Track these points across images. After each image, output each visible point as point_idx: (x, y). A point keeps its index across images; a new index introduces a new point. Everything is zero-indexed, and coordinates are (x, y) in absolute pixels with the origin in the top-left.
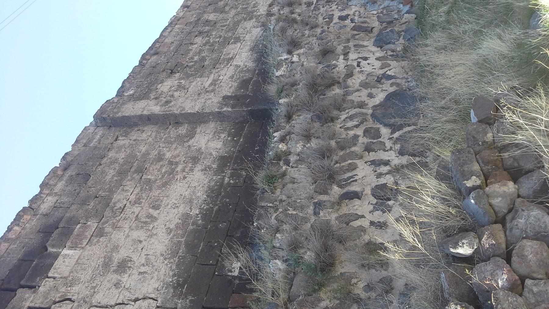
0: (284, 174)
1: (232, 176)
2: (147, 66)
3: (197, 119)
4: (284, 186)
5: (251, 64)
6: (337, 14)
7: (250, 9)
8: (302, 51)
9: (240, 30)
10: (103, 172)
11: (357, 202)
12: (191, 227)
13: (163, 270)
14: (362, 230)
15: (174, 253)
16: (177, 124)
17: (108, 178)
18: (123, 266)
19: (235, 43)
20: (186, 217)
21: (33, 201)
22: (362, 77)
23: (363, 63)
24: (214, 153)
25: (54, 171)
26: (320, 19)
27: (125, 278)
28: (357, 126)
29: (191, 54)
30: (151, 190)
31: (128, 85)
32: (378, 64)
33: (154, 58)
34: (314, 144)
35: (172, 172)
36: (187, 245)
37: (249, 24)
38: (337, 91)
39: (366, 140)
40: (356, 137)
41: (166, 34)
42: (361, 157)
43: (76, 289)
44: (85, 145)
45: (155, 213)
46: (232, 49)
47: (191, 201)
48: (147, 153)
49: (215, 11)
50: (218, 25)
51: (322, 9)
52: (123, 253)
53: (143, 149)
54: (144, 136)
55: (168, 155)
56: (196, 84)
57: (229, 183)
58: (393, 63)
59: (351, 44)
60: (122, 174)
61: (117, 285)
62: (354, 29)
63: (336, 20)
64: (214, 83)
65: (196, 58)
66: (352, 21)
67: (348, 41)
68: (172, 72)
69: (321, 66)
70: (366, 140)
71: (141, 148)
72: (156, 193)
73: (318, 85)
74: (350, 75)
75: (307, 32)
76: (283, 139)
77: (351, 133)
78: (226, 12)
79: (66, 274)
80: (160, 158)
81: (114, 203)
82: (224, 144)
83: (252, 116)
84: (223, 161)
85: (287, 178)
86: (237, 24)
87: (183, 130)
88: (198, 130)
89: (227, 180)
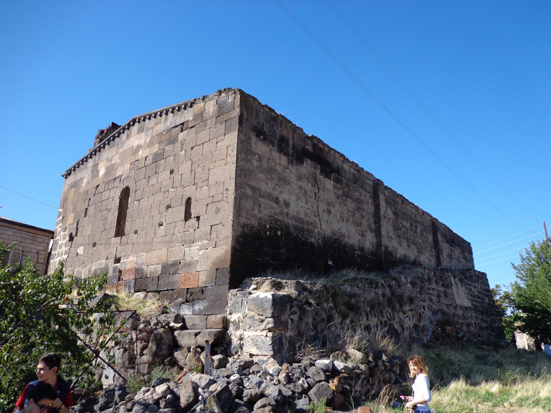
0: (372, 287)
1: (358, 254)
2: (397, 199)
3: (378, 232)
4: (369, 288)
5: (398, 256)
6: (425, 304)
7: (422, 250)
8: (411, 288)
9: (413, 247)
10: (357, 190)
11: (366, 318)
12: (341, 239)
13: (328, 230)
14: (360, 321)
15: (334, 234)
16: (375, 222)
17: (355, 194)
18: (329, 212)
19: (408, 245)
20: (343, 236)
21: (348, 160)
22: (402, 318)
23: (408, 318)
24: (365, 244)
25: (357, 165)
26: (423, 296)
27: (326, 214)
28: (387, 317)
29: (402, 222)
30: (352, 216)
31: (389, 191)
32: (408, 326)
33: (400, 202)
34: (381, 298)
35: (358, 225)
36: (336, 239)
37: (415, 251)
38: (398, 307)
39: (383, 321)
40: (384, 317)
41: (411, 205)
42: (378, 319)
43: (322, 192)
44: (366, 177)
45: (345, 221)
46: (405, 244)
47: (349, 237)
48: (364, 210)
49: (422, 231)
50: (415, 234)
51: (427, 296)
52: (333, 210)
53: (365, 208)
54: (370, 206)
55: (364, 221)
56: (391, 228)
57: (355, 254)
58: (408, 332)
59: (414, 312)
60: (357, 200)
61: (324, 211)
62: (420, 313)
63: (423, 304)
64: (391, 238)
65: (401, 225)
66: (423, 312)
67: (416, 311)
68: (395, 214)
69: (405, 298)
70: (383, 321)
71: (366, 206)
72: (351, 219)
73: (401, 300)
74: (404, 313)
75: (418, 290)
76: (382, 285)
77: (385, 315)
78: (421, 237)
79: (326, 186)
80: (363, 217)
81: (347, 201)
82: (369, 249)
83: (380, 262)
84: (362, 249)
85: (371, 289)
86: (415, 244)
87: (373, 226)
88: (373, 234)
89: (356, 252)
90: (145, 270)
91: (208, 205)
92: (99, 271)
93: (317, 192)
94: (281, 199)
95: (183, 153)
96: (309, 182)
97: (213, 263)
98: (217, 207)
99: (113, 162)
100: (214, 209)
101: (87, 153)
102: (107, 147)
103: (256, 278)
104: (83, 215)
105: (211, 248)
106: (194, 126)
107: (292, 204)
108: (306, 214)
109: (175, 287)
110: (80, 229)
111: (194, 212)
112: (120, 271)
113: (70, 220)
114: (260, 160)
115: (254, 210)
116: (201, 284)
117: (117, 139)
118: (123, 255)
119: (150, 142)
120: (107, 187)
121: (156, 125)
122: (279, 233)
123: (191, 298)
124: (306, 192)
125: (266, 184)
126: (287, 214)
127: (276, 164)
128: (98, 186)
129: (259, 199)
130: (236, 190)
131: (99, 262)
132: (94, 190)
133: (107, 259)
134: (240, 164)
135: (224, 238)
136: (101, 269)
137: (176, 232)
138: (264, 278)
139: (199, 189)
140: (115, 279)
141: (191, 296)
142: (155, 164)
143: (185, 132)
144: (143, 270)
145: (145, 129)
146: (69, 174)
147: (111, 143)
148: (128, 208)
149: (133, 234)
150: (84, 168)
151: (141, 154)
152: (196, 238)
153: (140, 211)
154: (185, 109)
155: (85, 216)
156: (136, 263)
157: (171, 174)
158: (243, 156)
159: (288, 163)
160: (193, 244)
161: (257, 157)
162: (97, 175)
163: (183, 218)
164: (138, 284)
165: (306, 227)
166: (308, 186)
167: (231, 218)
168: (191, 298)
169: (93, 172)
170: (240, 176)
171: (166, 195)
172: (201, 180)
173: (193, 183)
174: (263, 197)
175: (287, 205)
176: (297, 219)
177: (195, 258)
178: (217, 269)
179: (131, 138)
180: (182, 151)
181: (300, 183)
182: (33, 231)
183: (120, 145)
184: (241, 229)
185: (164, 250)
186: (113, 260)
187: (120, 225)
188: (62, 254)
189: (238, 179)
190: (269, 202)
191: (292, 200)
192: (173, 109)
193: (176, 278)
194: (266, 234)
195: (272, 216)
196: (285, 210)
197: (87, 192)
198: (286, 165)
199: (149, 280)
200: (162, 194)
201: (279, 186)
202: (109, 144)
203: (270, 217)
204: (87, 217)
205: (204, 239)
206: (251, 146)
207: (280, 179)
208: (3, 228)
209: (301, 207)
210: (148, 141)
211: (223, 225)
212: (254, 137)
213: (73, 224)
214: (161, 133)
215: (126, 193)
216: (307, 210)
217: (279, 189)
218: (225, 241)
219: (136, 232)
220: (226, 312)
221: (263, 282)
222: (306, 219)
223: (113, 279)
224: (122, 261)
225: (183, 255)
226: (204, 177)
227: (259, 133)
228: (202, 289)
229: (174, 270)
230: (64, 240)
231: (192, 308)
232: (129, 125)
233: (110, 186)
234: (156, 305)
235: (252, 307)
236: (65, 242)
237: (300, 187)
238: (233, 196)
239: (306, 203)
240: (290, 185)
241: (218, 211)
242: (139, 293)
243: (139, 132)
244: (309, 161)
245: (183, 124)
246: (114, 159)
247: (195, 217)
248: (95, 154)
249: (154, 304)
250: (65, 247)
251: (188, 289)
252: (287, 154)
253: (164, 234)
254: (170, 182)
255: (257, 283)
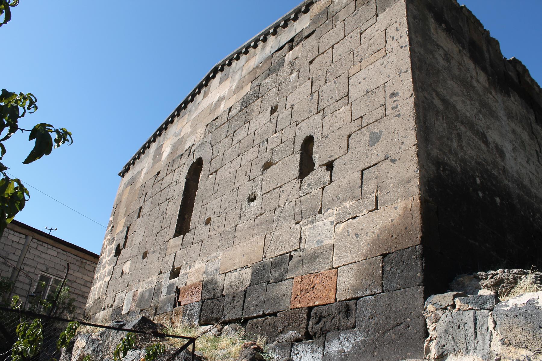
90: (220, 283)
91: (349, 136)
92: (147, 294)
93: (538, 150)
94: (490, 140)
95: (295, 75)
96: (524, 129)
97: (374, 243)
98: (372, 133)
99: (182, 135)
100: (366, 138)
101: (149, 136)
102: (176, 120)
103: (492, 272)
104: (136, 217)
105: (365, 212)
106: (314, 32)
107: (507, 155)
108: (531, 181)
109: (281, 308)
110: (130, 236)
111: (319, 157)
112: (178, 291)
113: (121, 227)
114: (447, 57)
115: (452, 140)
116: (343, 294)
117: (190, 106)
118: (184, 262)
119: (237, 87)
120: (170, 169)
121: (246, 62)
122: (498, 200)
123: (318, 327)
124: (523, 142)
125: (463, 102)
126: (504, 170)
127: (471, 77)
128: (159, 173)
129: (458, 125)
130: (415, 88)
131: (148, 280)
132: (154, 178)
133: (161, 273)
134: (416, 49)
135: (397, 185)
136: (150, 291)
137: (282, 202)
138: (515, 270)
139: (329, 116)
140: (169, 305)
141: (317, 324)
142: (245, 110)
143: (296, 49)
144: (216, 283)
145: (230, 75)
146: (127, 170)
147: (182, 114)
148: (197, 188)
149: (203, 225)
150: (145, 157)
151: (223, 107)
152: (325, 201)
153: (216, 186)
154: (295, 19)
155: (139, 217)
156: (206, 272)
157: (271, 114)
158: (420, 39)
159: (490, 85)
160: (318, 216)
161: (441, 52)
162: (160, 160)
163: (296, 173)
164: (206, 309)
165: (536, 205)
166: (525, 136)
167: (412, 138)
168: (318, 327)
169: (154, 157)
170: (420, 69)
171: (262, 148)
172: (331, 101)
173: (316, 112)
174: (462, 123)
175: (502, 154)
176: (521, 186)
177: (327, 242)
178: (384, 256)
179: (210, 94)
180: (291, 73)
181: (513, 125)
182: (81, 254)
183: (193, 111)
184: (433, 168)
185: (258, 240)
186: (168, 274)
187: (184, 219)
188: (104, 276)
189: (417, 73)
190: (471, 134)
191: (508, 147)
192: (276, 27)
193: (283, 288)
194: (478, 194)
195: (483, 165)
196: (499, 160)
197: (144, 186)
198: (487, 85)
199: (226, 299)
200: (256, 149)
201: (484, 116)
202: (178, 115)
203: (478, 163)
204: (141, 217)
205: (345, 200)
206: (429, 29)
207: (483, 104)
208: (46, 245)
209: (523, 166)
210: (234, 87)
211: (393, 161)
212: (433, 21)
213: (122, 232)
214: (256, 68)
215: (196, 168)
216: (531, 174)
217: (484, 121)
218: (401, 189)
219: (208, 221)
220: (428, 351)
221: (516, 280)
222: (532, 190)
223: (166, 304)
224: (182, 272)
225: (296, 241)
226: (338, 94)
227: (439, 19)
228: (347, 306)
229: (278, 273)
230: (108, 256)
231: (320, 349)
232: (208, 79)
233: (174, 166)
234: (240, 344)
235: (518, 334)
236: (110, 258)
237: (514, 131)
238: (412, 100)
239: (528, 162)
240: (499, 120)
241: (375, 139)
242: (207, 327)
243: (221, 82)
244: (517, 97)
245: (292, 40)
246: (183, 130)
247: (321, 166)
248: (160, 135)
249: (234, 344)
250: (109, 265)
251: (310, 309)
252: (484, 69)
253: (258, 213)
254: (271, 124)
255: (497, 284)
